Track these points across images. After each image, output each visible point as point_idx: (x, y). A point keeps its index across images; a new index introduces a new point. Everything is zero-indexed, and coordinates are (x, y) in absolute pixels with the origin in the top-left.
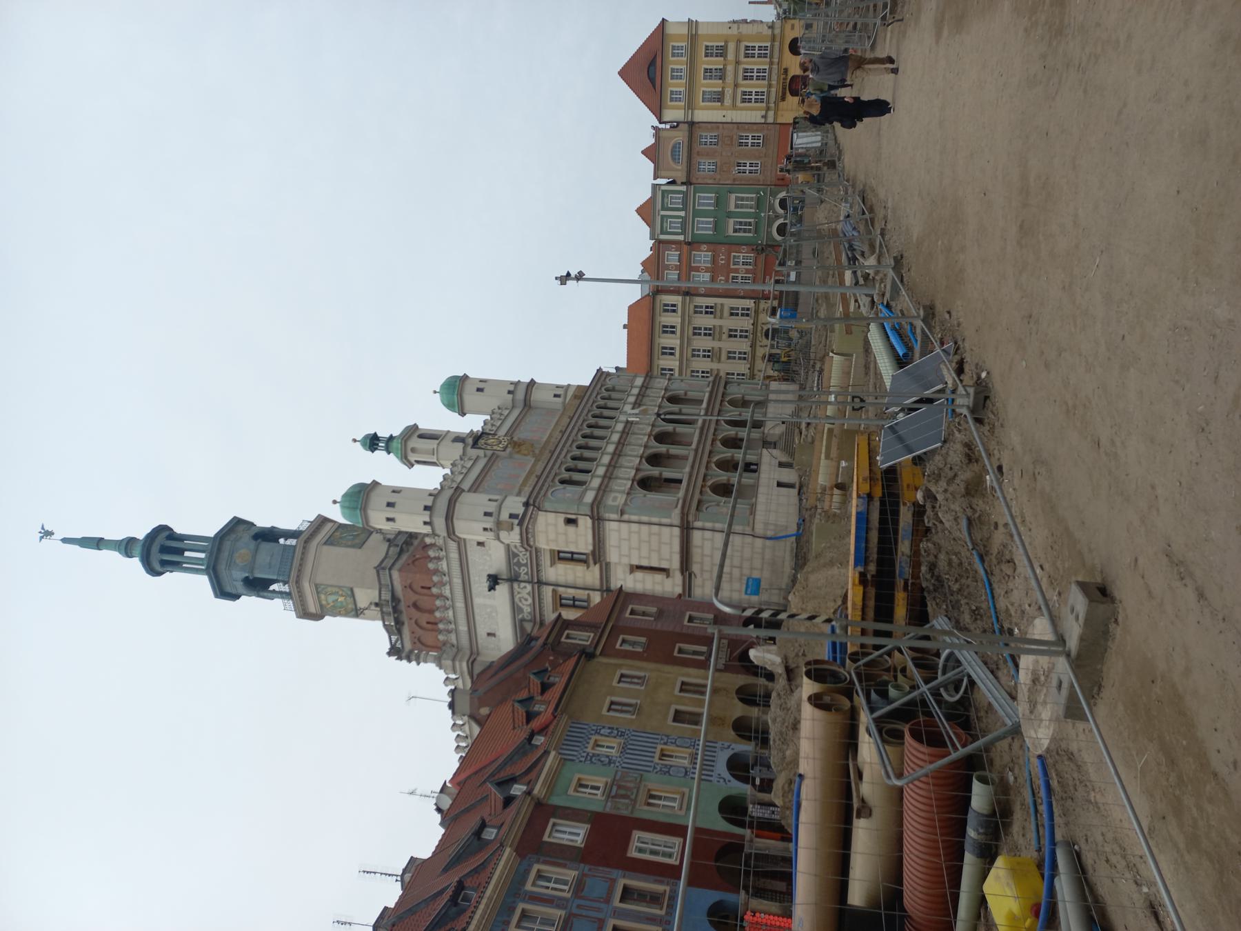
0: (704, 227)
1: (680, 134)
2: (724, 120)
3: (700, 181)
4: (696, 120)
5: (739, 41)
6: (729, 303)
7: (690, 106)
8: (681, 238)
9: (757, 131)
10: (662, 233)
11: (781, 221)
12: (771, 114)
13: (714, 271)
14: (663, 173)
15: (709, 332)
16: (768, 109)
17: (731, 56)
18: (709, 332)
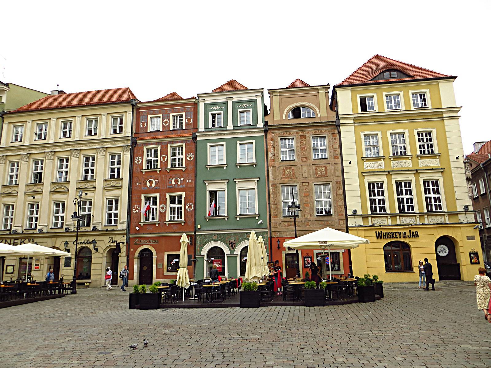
0: (216, 156)
1: (324, 114)
2: (345, 164)
3: (270, 142)
4: (342, 129)
5: (442, 170)
6: (123, 195)
7: (357, 121)
8: (201, 128)
9: (337, 207)
10: (206, 105)
11: (227, 251)
12: (360, 221)
13: (164, 174)
14: (276, 99)
15: (88, 176)
16: (365, 217)
17: (423, 163)
18: (88, 176)
